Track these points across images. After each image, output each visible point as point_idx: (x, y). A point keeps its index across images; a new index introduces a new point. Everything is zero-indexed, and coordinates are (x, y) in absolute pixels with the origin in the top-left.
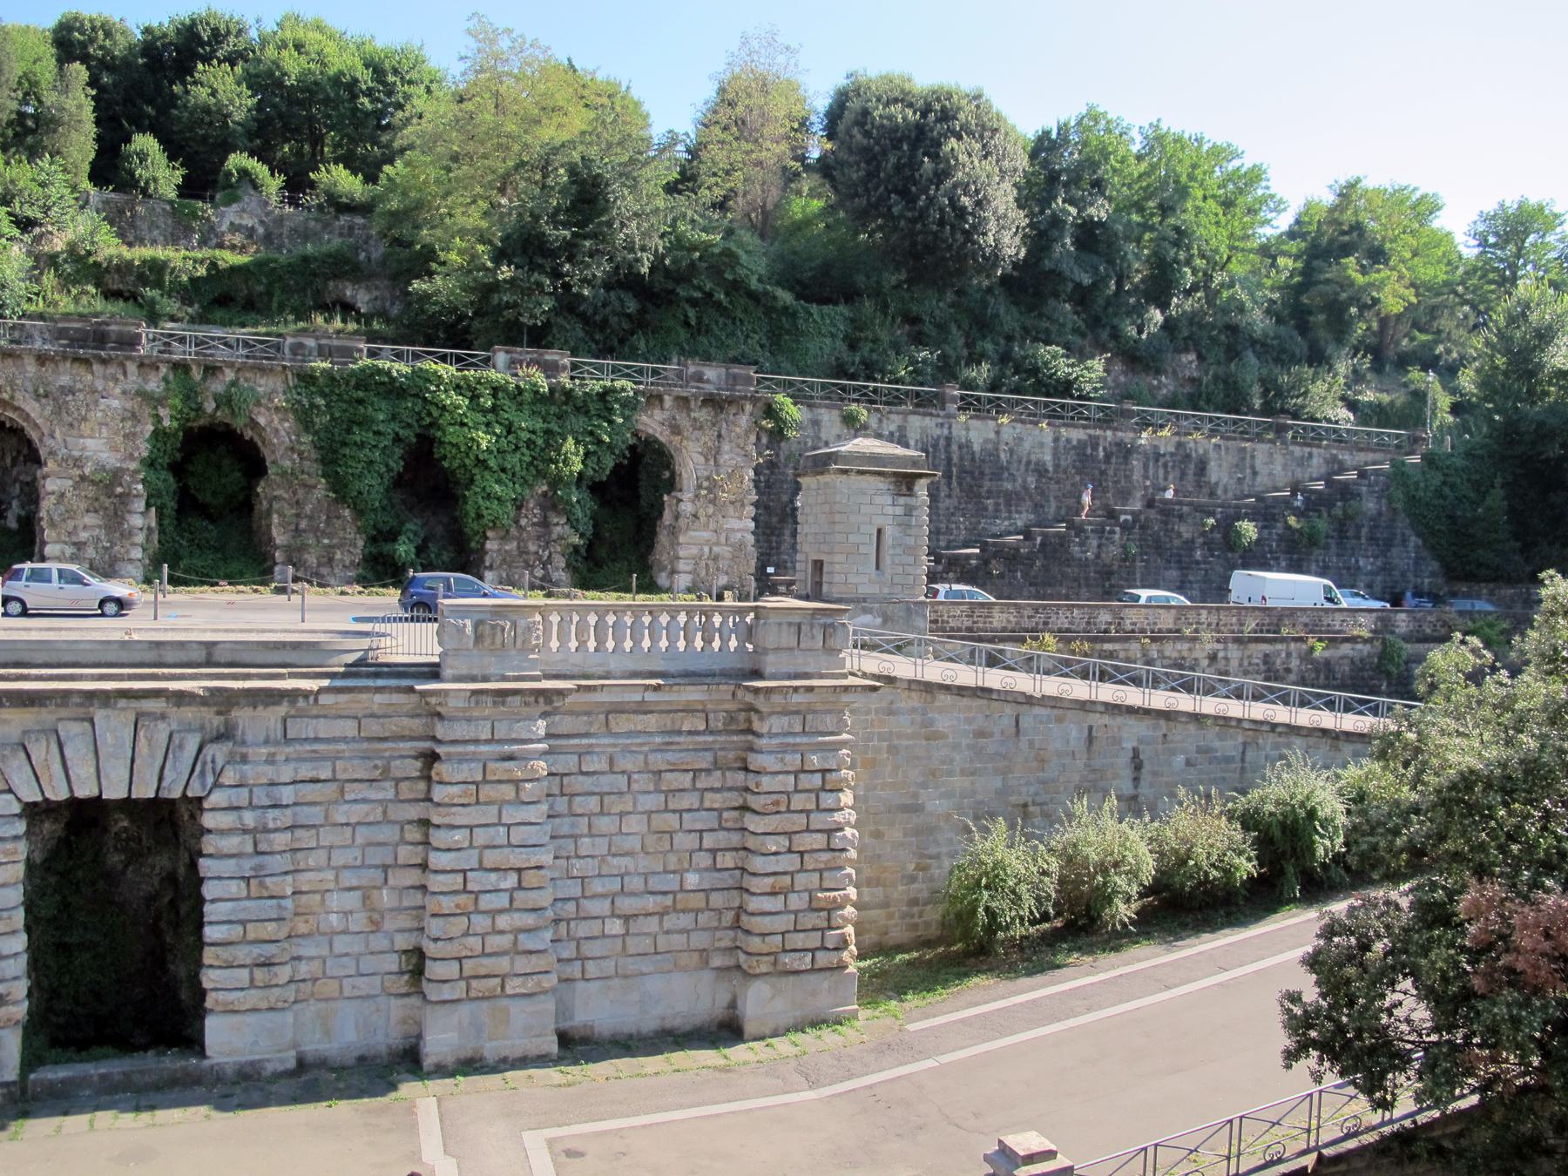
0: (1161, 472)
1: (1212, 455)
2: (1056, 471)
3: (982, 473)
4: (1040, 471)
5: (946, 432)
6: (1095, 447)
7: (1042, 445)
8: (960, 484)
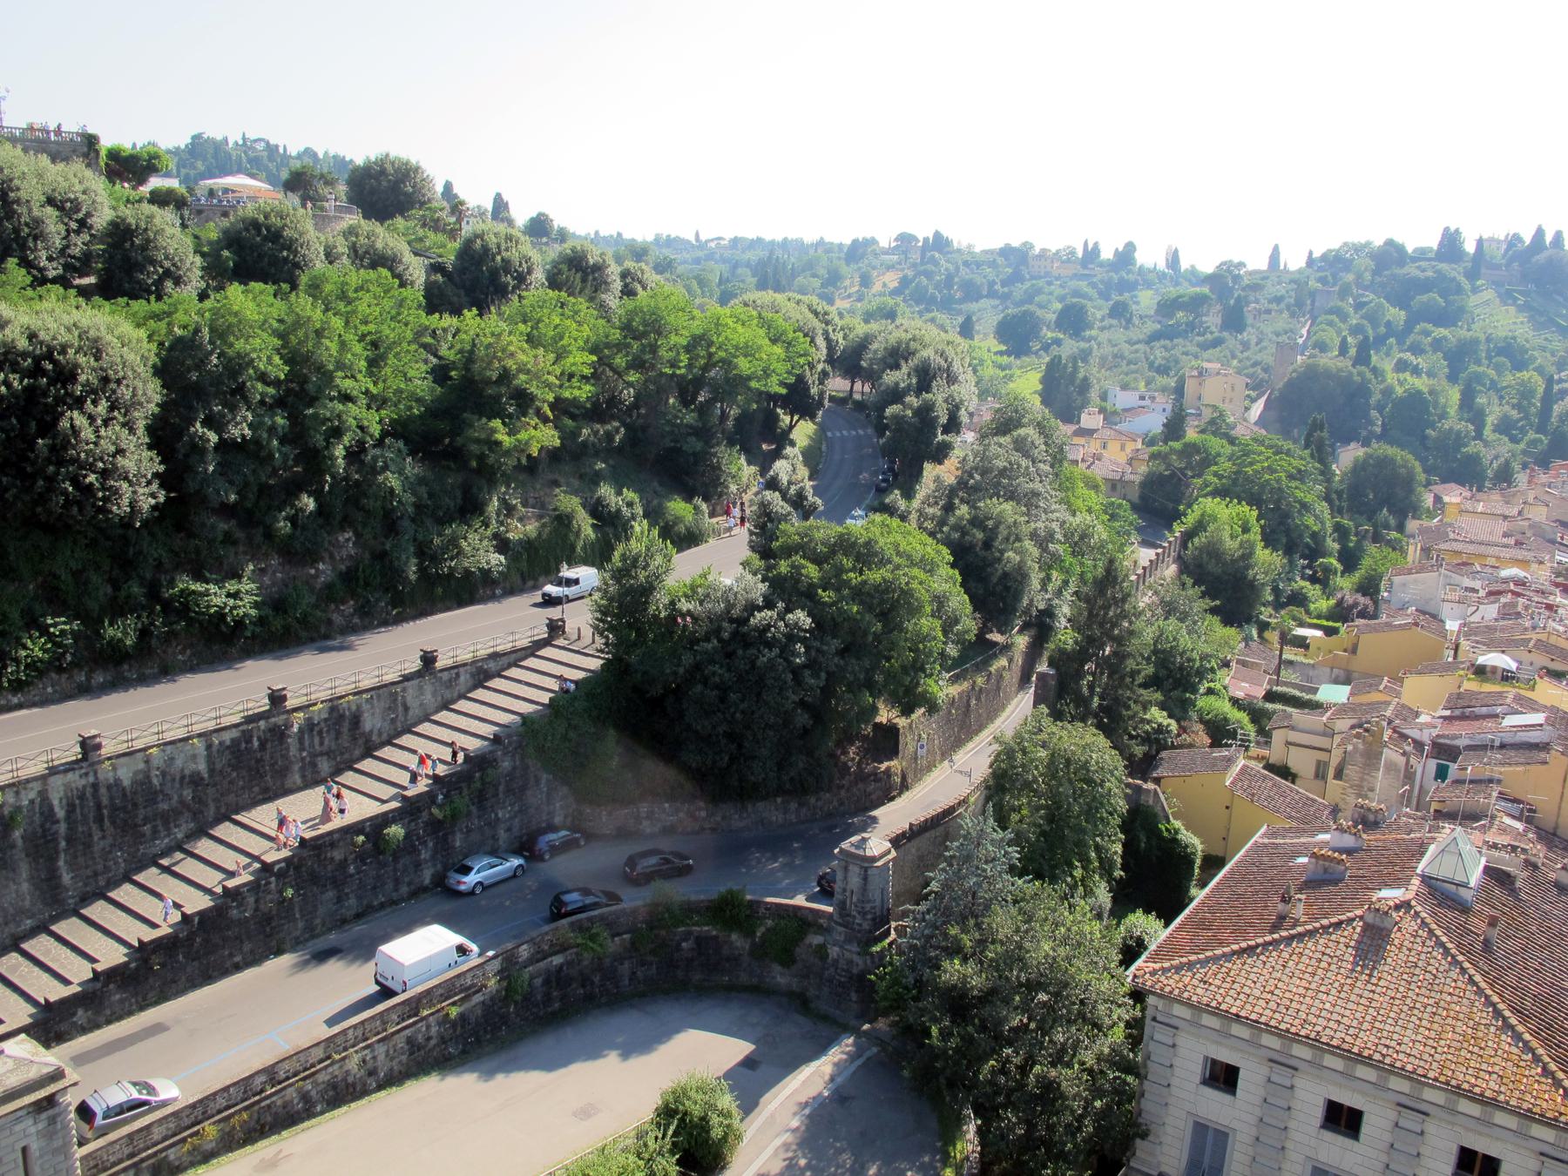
0: (317, 740)
1: (365, 707)
2: (211, 776)
3: (135, 805)
4: (195, 780)
5: (91, 779)
6: (249, 741)
7: (194, 757)
8: (113, 823)
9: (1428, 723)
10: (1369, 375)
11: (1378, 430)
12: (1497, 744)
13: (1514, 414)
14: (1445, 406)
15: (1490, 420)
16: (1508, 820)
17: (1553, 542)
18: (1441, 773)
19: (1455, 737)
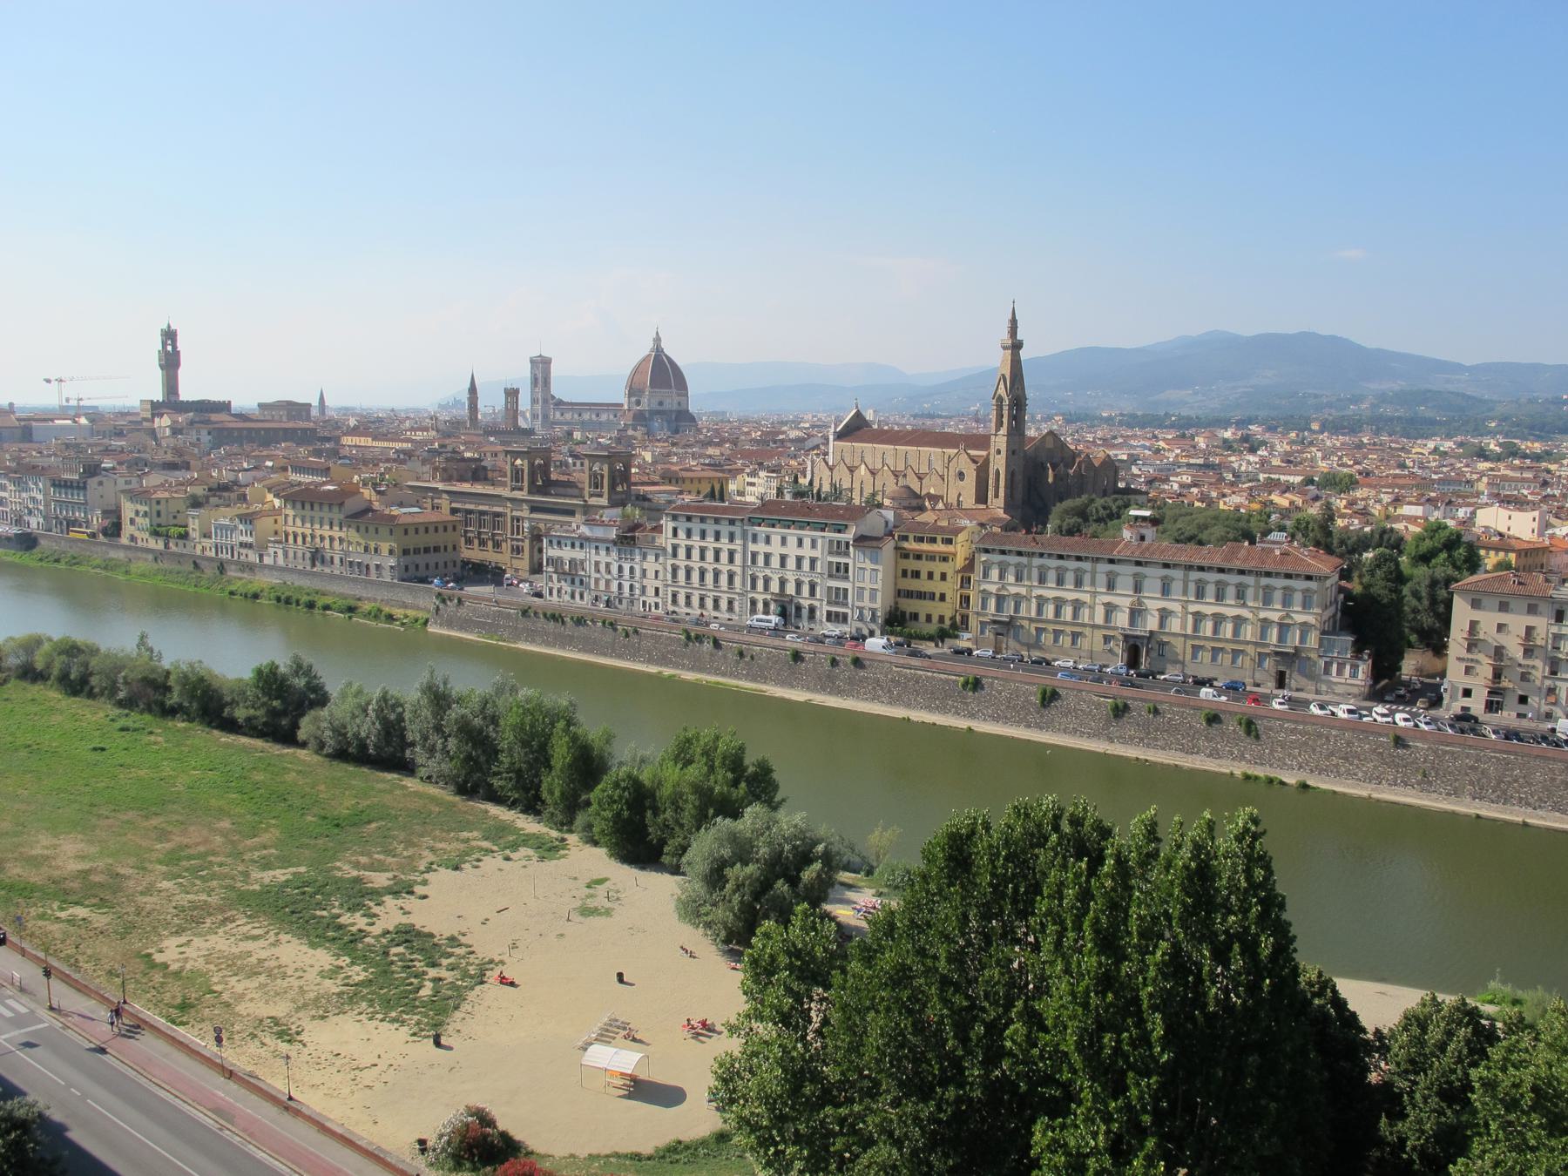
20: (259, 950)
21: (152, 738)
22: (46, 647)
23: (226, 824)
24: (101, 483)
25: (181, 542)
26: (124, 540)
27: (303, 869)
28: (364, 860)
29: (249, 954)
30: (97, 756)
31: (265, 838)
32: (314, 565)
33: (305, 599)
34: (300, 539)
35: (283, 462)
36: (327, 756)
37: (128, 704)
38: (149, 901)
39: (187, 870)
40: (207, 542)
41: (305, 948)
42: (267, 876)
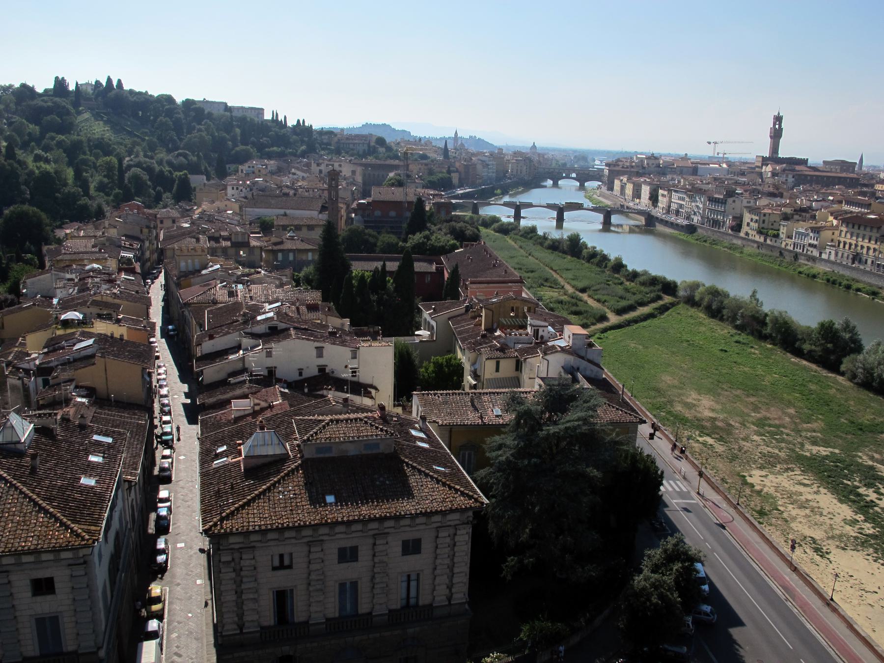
9: (36, 357)
10: (16, 165)
11: (28, 196)
12: (72, 360)
13: (106, 180)
14: (65, 179)
15: (92, 186)
16: (79, 400)
17: (120, 246)
18: (46, 383)
19: (49, 362)
20: (807, 494)
21: (753, 350)
22: (701, 289)
23: (792, 411)
24: (734, 201)
25: (774, 239)
26: (742, 234)
27: (837, 451)
28: (877, 456)
29: (801, 494)
30: (723, 355)
31: (814, 425)
32: (853, 263)
33: (845, 282)
34: (847, 247)
35: (840, 198)
36: (857, 384)
37: (741, 328)
38: (747, 445)
39: (768, 432)
40: (789, 241)
41: (835, 501)
42: (815, 449)
